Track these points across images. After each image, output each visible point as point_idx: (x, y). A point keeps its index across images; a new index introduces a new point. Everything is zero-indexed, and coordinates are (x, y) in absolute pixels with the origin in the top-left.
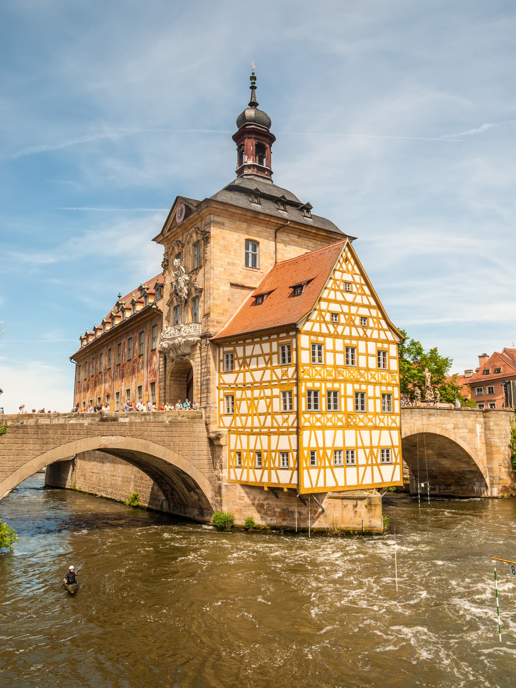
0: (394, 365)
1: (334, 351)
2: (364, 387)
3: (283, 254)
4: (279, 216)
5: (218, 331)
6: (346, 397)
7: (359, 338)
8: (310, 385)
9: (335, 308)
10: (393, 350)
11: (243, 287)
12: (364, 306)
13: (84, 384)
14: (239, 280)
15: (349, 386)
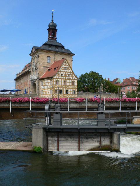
0: (76, 84)
1: (61, 82)
2: (68, 89)
3: (56, 59)
4: (56, 51)
5: (41, 77)
6: (64, 91)
7: (68, 79)
8: (55, 89)
9: (62, 73)
10: (76, 81)
11: (46, 67)
12: (69, 72)
13: (17, 86)
14: (46, 66)
15: (65, 89)
